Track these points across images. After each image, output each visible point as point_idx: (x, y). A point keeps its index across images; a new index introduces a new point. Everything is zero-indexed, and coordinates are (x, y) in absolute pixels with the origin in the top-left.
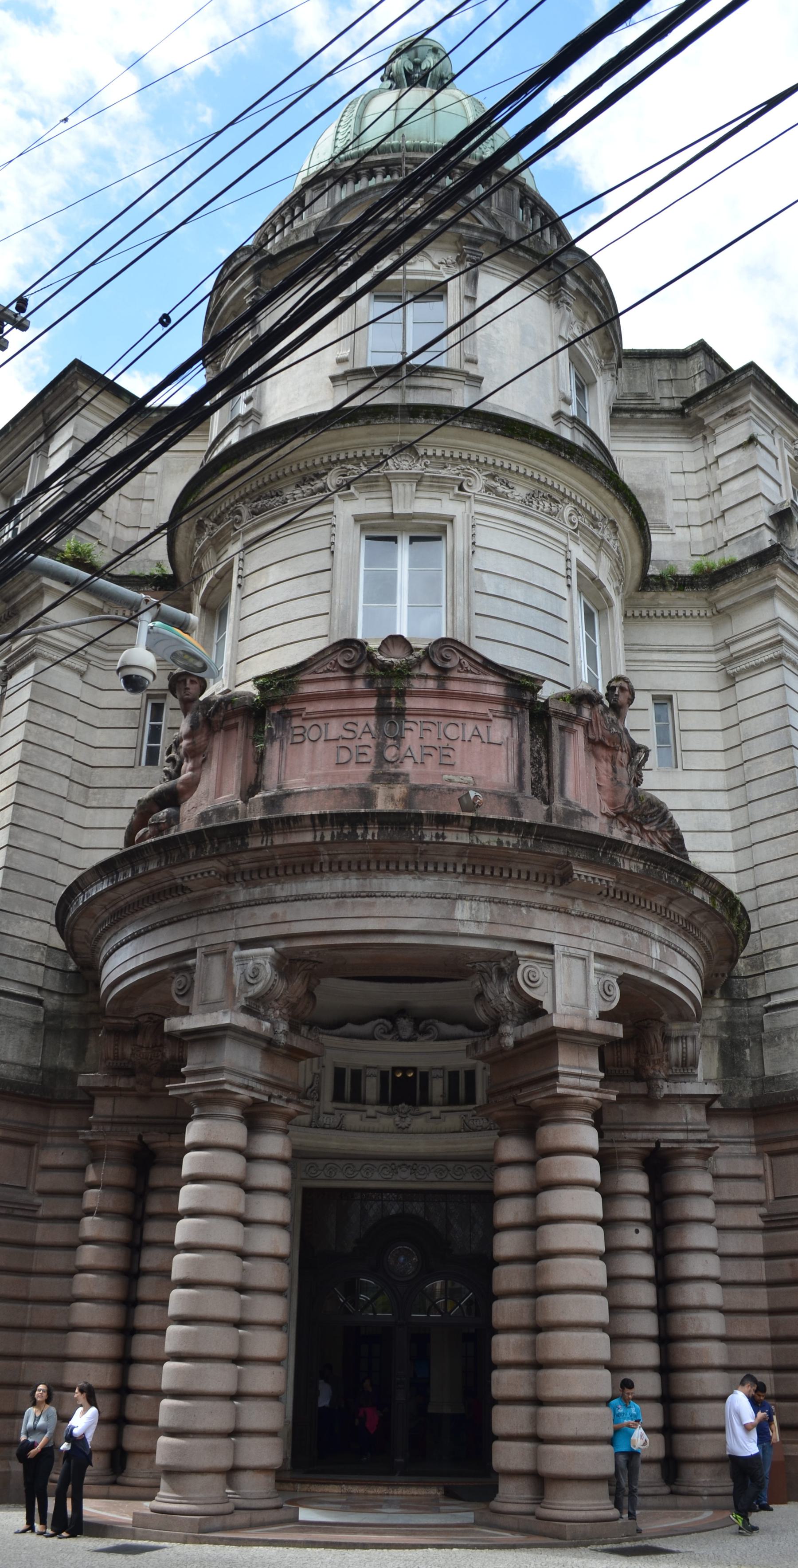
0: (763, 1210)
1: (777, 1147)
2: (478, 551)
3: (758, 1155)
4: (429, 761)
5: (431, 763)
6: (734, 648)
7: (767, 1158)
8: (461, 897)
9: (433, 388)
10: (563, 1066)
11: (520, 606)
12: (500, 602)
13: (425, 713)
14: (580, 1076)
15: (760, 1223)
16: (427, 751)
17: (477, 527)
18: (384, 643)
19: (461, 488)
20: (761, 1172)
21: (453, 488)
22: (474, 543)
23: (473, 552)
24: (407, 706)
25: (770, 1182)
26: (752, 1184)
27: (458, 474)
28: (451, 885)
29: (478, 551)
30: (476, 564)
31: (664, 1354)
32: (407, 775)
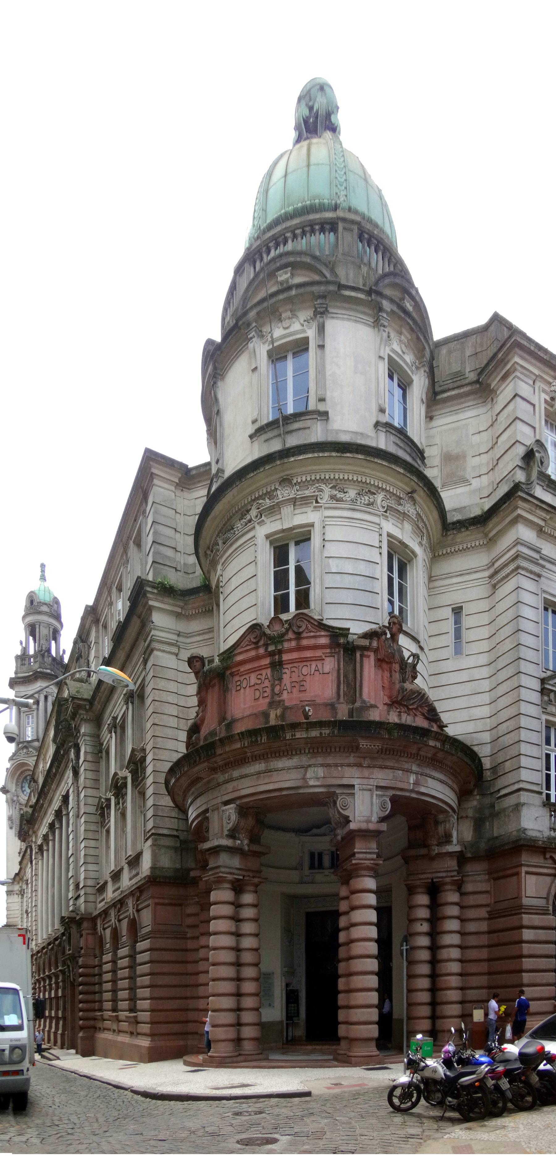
0: (489, 909)
1: (496, 875)
2: (327, 544)
3: (488, 880)
4: (295, 690)
5: (295, 690)
6: (497, 565)
7: (492, 881)
8: (310, 766)
9: (300, 429)
10: (358, 849)
11: (350, 576)
12: (338, 577)
13: (292, 661)
14: (366, 853)
15: (487, 916)
16: (293, 685)
17: (326, 527)
18: (271, 622)
19: (317, 502)
20: (489, 889)
21: (312, 503)
22: (324, 540)
23: (324, 546)
24: (283, 659)
25: (492, 894)
26: (484, 896)
27: (314, 492)
28: (304, 760)
29: (327, 544)
30: (326, 554)
31: (433, 983)
32: (284, 701)
